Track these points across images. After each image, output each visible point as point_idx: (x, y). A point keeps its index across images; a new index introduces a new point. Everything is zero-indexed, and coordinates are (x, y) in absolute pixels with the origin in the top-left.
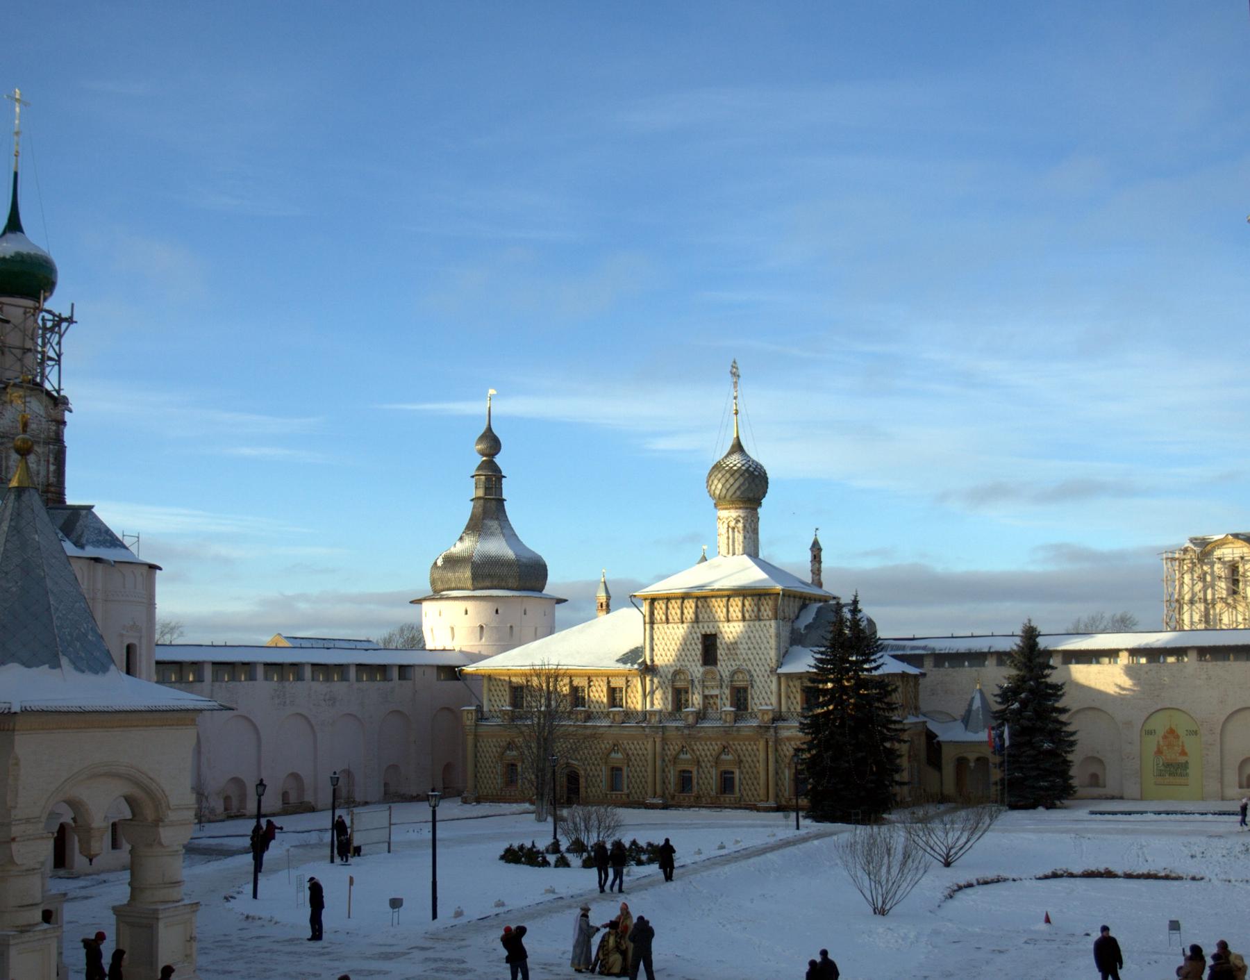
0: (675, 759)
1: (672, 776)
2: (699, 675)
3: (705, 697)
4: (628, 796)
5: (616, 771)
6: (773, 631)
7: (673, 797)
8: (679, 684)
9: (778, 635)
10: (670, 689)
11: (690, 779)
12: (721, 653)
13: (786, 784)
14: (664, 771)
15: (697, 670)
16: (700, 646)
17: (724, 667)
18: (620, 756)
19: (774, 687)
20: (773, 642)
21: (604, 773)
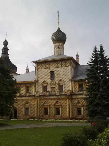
0: (43, 105)
1: (42, 110)
2: (50, 82)
3: (51, 88)
4: (30, 116)
5: (27, 109)
6: (70, 69)
7: (42, 116)
8: (44, 85)
9: (71, 70)
10: (42, 86)
11: (47, 111)
12: (56, 76)
13: (75, 111)
14: (40, 109)
15: (49, 81)
16: (50, 75)
17: (56, 80)
18: (28, 105)
19: (70, 84)
20: (70, 72)
21: (24, 110)
